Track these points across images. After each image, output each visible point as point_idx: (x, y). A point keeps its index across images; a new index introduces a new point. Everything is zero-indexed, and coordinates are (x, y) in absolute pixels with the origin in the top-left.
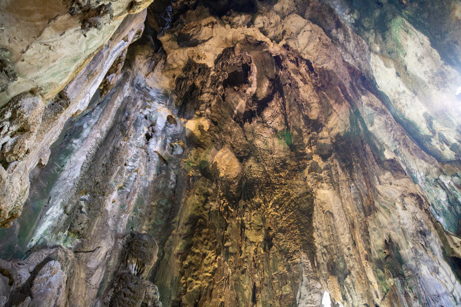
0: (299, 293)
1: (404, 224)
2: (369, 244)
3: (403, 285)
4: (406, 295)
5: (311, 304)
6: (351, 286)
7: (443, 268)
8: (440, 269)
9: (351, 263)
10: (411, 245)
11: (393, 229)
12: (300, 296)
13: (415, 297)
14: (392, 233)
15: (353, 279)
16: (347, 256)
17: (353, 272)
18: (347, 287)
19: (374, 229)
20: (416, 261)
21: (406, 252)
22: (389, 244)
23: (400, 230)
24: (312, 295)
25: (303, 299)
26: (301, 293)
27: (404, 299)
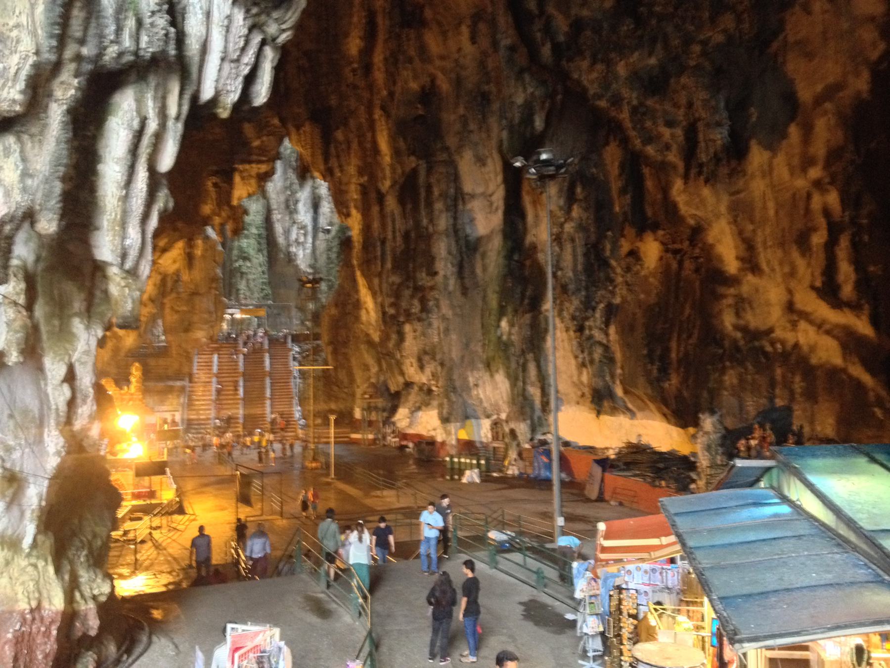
1: (463, 67)
2: (394, 83)
3: (429, 171)
4: (429, 188)
6: (344, 146)
8: (489, 161)
9: (353, 103)
10: (461, 111)
11: (443, 70)
13: (440, 195)
14: (440, 75)
15: (351, 136)
16: (348, 86)
17: (352, 123)
18: (336, 148)
19: (410, 60)
20: (461, 140)
21: (450, 118)
22: (428, 95)
23: (453, 76)
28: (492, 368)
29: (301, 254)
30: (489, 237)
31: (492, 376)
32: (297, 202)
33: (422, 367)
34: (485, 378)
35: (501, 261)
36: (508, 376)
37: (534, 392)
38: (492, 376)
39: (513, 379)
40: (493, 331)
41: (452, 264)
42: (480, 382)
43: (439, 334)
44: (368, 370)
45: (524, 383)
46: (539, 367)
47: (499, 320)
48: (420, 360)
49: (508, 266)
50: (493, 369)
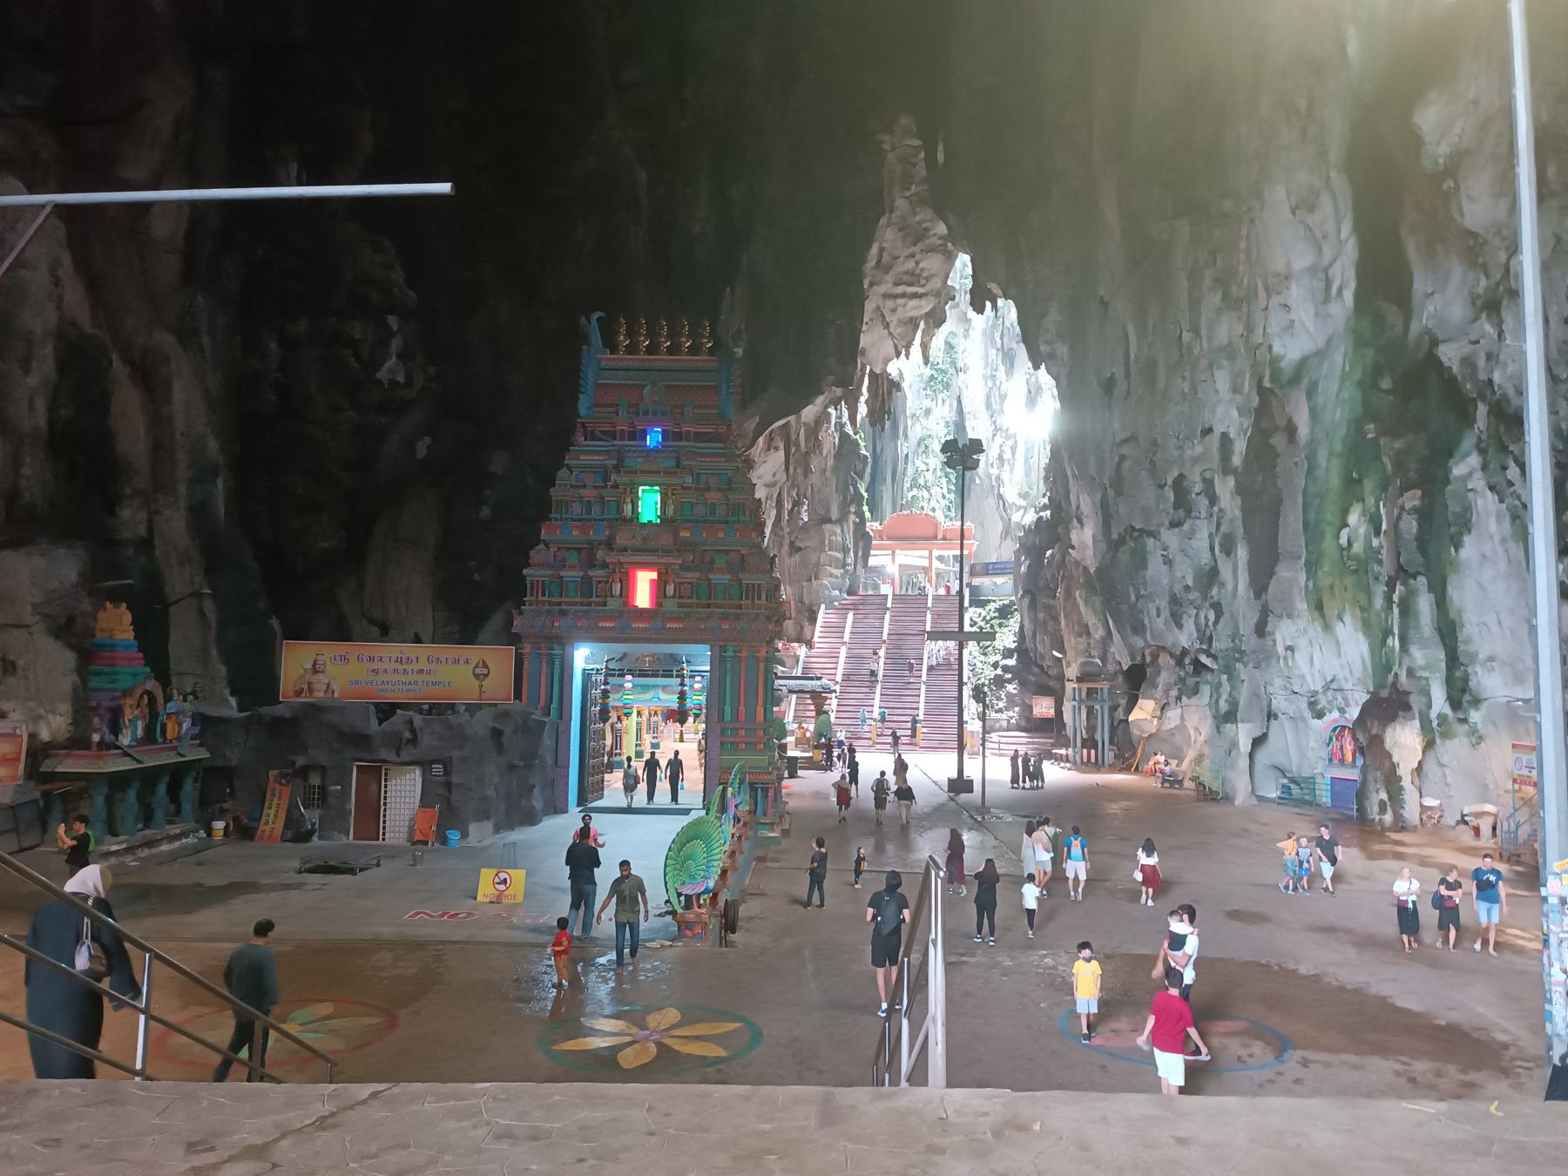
0: (874, 250)
5: (911, 284)
7: (1334, 198)
12: (879, 261)
13: (1217, 280)
24: (918, 257)
26: (882, 250)
27: (1184, 284)
28: (1326, 610)
29: (1005, 476)
30: (1321, 354)
31: (1327, 627)
32: (1003, 398)
33: (1177, 620)
34: (1311, 632)
35: (1351, 393)
36: (1367, 626)
37: (1426, 656)
38: (1327, 627)
39: (1378, 636)
40: (1329, 536)
41: (1238, 409)
42: (1302, 643)
43: (1212, 549)
44: (1089, 634)
45: (1404, 640)
46: (1441, 602)
47: (1345, 512)
48: (1175, 601)
49: (1366, 402)
50: (1331, 609)
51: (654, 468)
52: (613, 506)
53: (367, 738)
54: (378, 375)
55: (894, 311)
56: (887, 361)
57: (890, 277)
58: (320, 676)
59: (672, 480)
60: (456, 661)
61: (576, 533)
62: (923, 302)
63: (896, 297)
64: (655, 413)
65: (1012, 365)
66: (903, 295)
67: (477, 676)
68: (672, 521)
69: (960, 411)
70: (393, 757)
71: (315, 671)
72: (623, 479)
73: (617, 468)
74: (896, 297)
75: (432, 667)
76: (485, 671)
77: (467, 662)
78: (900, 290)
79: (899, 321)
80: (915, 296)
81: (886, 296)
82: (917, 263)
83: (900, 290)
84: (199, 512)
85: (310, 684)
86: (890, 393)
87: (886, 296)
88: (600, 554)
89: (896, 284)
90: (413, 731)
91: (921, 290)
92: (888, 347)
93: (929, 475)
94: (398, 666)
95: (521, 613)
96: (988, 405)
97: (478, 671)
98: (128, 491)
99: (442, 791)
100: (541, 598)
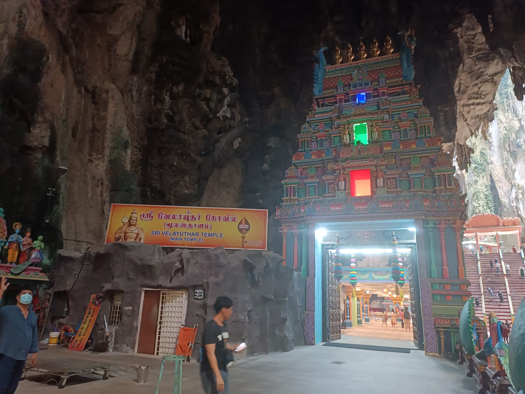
0: (457, 83)
5: (477, 98)
24: (479, 85)
25: (464, 92)
26: (460, 84)
32: (514, 172)
51: (363, 111)
52: (337, 139)
53: (150, 268)
54: (218, 115)
55: (468, 112)
56: (466, 139)
57: (465, 96)
58: (133, 228)
59: (375, 117)
60: (227, 219)
61: (314, 157)
62: (484, 106)
63: (470, 105)
64: (361, 85)
65: (516, 158)
66: (473, 104)
67: (241, 230)
68: (376, 142)
69: (492, 181)
70: (168, 284)
71: (130, 225)
72: (343, 121)
73: (338, 118)
74: (470, 105)
75: (210, 223)
76: (246, 226)
77: (234, 220)
78: (471, 102)
79: (472, 117)
80: (479, 104)
81: (464, 106)
82: (479, 88)
83: (471, 102)
84: (115, 164)
85: (125, 233)
86: (469, 154)
87: (464, 106)
88: (330, 166)
89: (469, 99)
90: (181, 261)
91: (482, 101)
92: (467, 131)
93: (480, 208)
94: (185, 221)
95: (280, 207)
96: (506, 176)
97: (241, 226)
98: (40, 119)
99: (201, 312)
100: (292, 198)
